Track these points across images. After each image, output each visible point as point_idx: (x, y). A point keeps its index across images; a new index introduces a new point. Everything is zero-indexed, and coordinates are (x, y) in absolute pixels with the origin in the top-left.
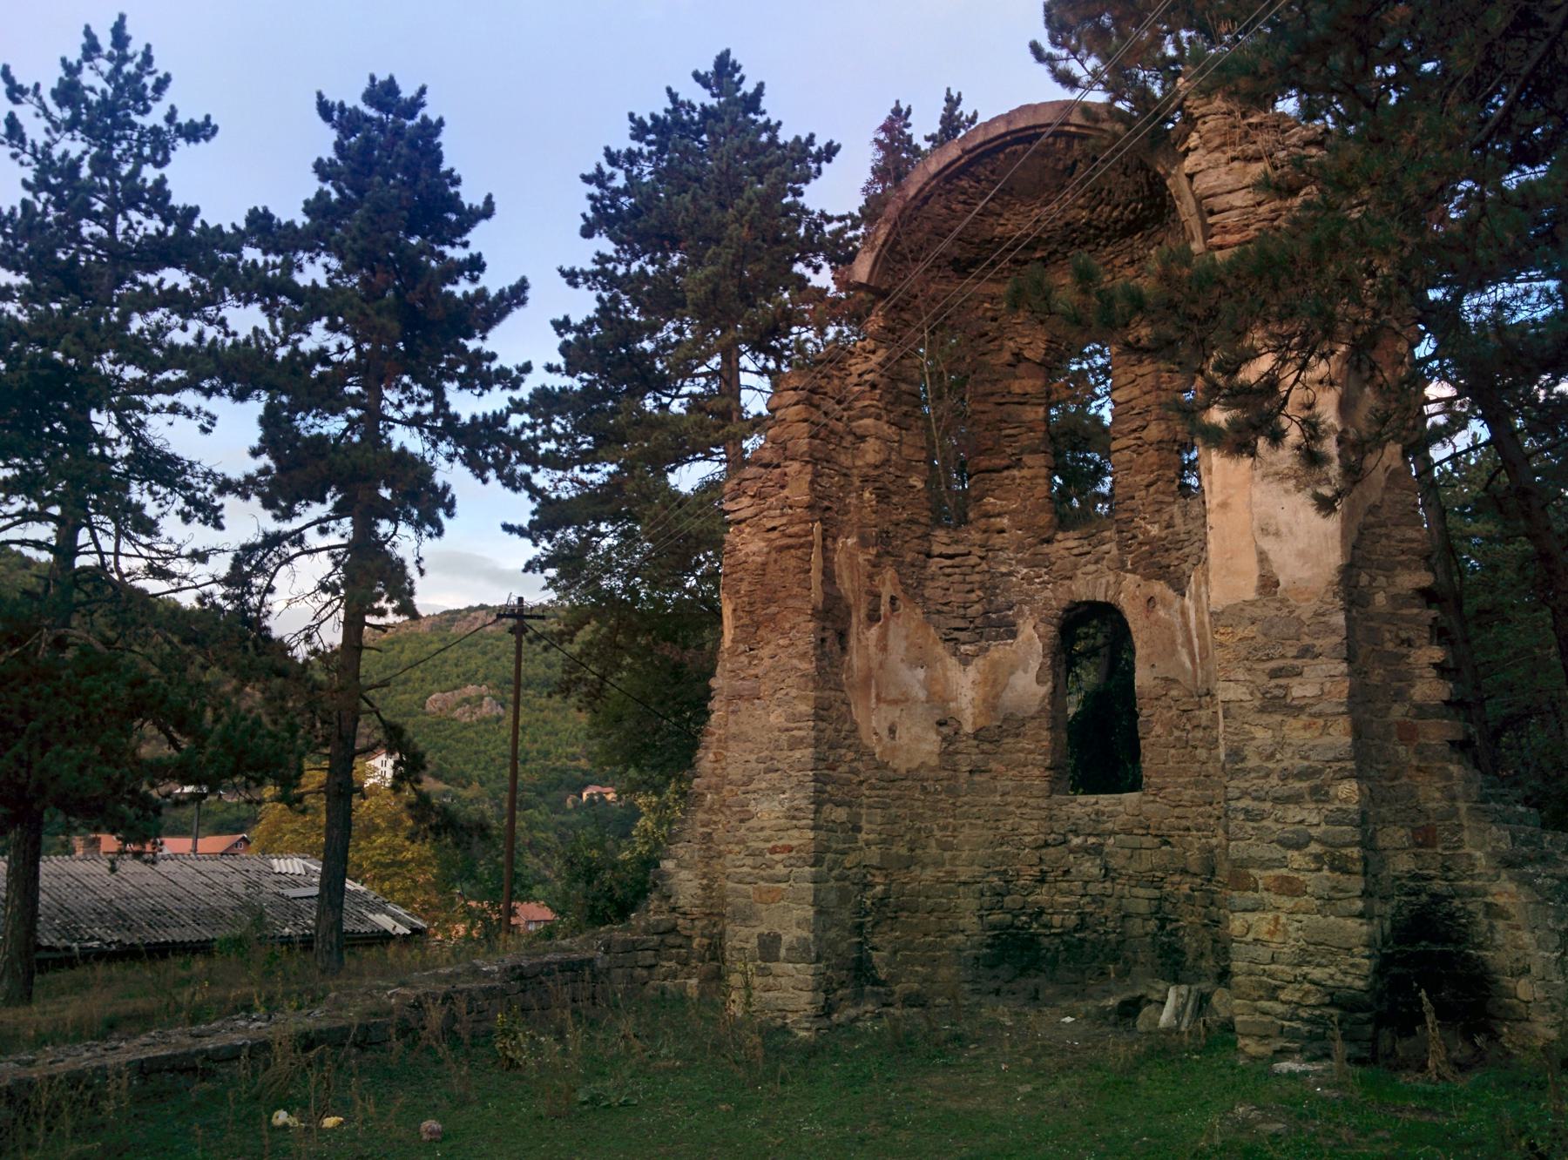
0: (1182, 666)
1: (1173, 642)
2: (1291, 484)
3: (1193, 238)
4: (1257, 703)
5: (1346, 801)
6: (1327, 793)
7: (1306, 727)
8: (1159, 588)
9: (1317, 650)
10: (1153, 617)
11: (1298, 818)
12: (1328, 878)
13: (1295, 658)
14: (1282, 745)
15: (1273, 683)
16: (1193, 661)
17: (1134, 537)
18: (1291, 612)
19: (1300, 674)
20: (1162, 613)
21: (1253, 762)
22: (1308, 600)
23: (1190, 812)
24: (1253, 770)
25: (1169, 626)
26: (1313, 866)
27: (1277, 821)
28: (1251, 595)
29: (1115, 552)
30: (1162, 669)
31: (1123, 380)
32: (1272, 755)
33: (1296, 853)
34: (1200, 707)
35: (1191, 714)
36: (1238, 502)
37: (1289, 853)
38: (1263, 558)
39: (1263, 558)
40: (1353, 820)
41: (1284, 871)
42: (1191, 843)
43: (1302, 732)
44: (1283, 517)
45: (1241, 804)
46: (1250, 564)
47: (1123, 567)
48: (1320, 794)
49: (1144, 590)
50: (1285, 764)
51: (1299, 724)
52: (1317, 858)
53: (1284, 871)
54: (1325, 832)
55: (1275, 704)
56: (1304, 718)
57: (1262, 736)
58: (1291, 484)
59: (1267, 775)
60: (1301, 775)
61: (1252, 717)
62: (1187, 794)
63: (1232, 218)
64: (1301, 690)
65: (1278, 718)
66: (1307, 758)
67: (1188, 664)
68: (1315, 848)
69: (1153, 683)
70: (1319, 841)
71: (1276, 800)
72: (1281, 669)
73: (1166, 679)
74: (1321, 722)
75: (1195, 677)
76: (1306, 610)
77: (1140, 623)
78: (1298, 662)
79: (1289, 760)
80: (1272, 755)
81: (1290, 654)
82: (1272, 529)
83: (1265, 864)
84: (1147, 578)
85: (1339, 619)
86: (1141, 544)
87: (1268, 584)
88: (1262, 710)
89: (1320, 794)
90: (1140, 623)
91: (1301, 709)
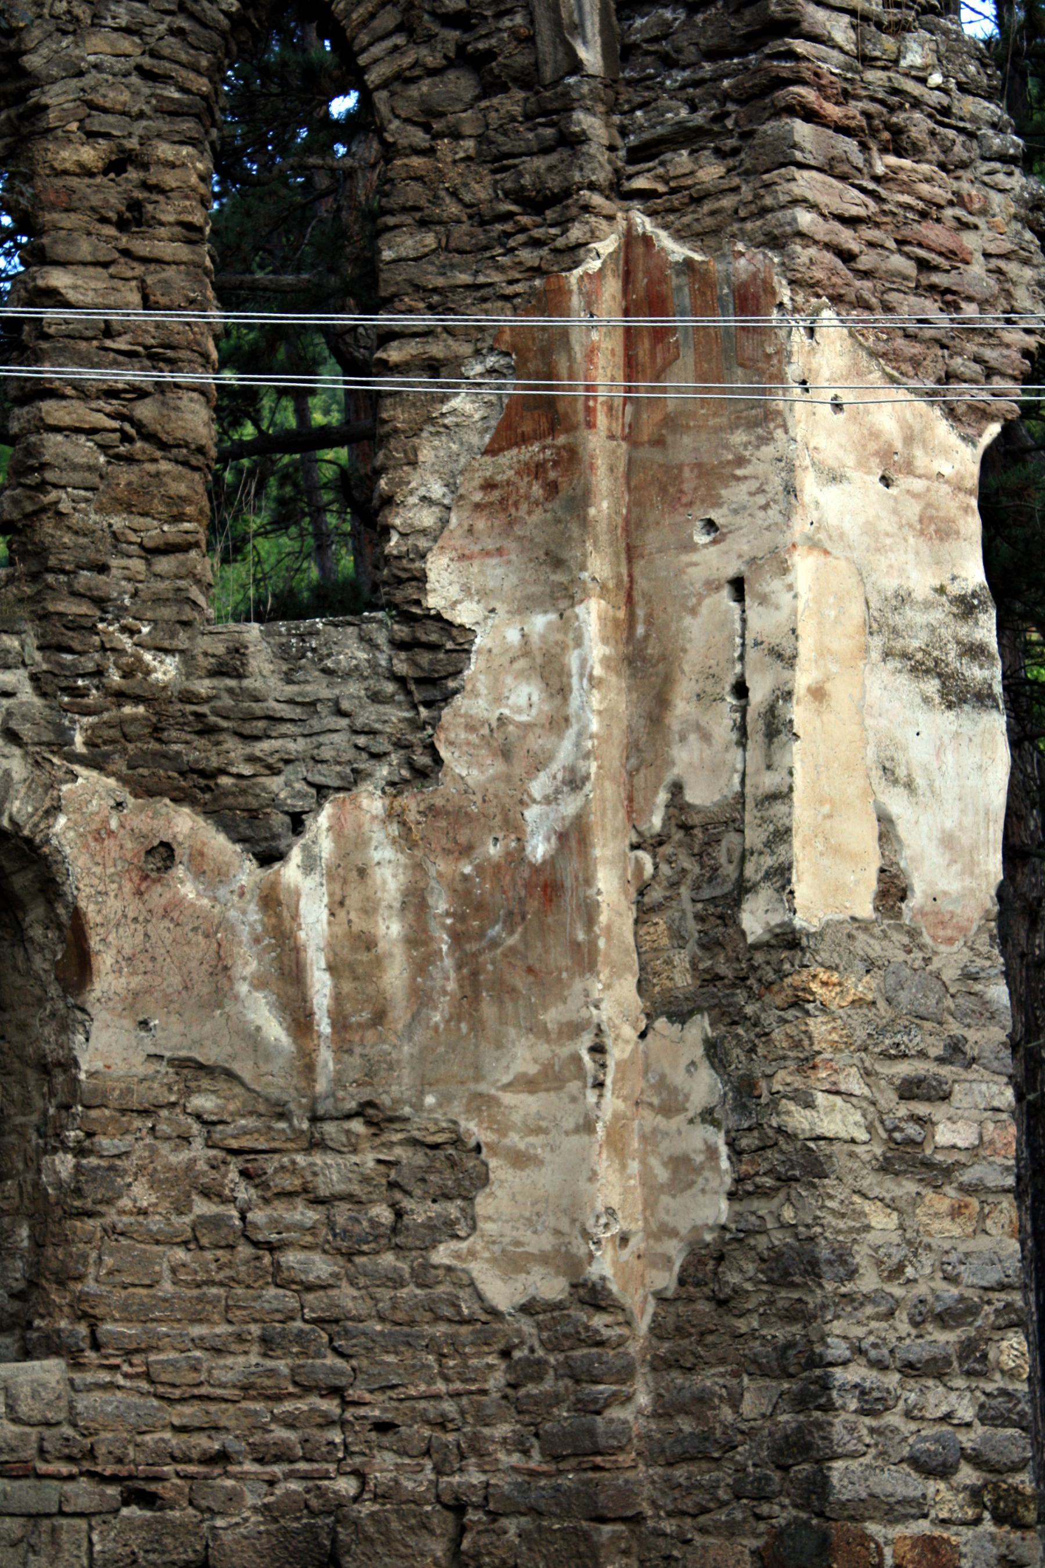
0: (253, 1038)
1: (221, 968)
2: (932, 686)
3: (578, 28)
4: (878, 1150)
5: (1012, 1374)
6: (985, 1356)
7: (956, 1212)
8: (184, 823)
9: (971, 1051)
10: (158, 896)
11: (944, 1409)
12: (993, 1538)
13: (941, 1060)
14: (915, 1247)
15: (903, 1110)
16: (300, 1022)
17: (99, 673)
18: (927, 960)
19: (946, 1097)
20: (189, 891)
21: (868, 1282)
22: (950, 941)
23: (225, 1415)
24: (868, 1298)
25: (215, 930)
26: (970, 1513)
27: (908, 1415)
28: (866, 910)
29: (27, 693)
30: (173, 1035)
31: (84, 248)
32: (900, 1269)
33: (942, 1486)
34: (316, 1144)
35: (270, 1165)
36: (840, 691)
37: (933, 1486)
38: (886, 829)
39: (886, 829)
40: (1022, 1415)
41: (923, 1526)
42: (233, 1497)
43: (947, 1223)
44: (918, 754)
45: (855, 1374)
46: (863, 834)
47: (60, 743)
48: (973, 1358)
49: (141, 822)
50: (922, 1289)
51: (943, 1205)
52: (975, 1494)
53: (923, 1526)
54: (985, 1440)
55: (905, 1155)
56: (950, 1190)
57: (882, 1222)
58: (932, 686)
59: (891, 1314)
60: (945, 1319)
61: (869, 1181)
62: (244, 1362)
63: (831, 64)
64: (951, 1133)
65: (910, 1187)
66: (952, 1279)
67: (275, 1030)
68: (967, 1475)
69: (142, 1069)
70: (976, 1460)
71: (910, 1369)
72: (919, 1082)
73: (181, 1064)
74: (974, 1203)
75: (309, 1069)
76: (950, 959)
77: (113, 905)
78: (945, 1071)
79: (926, 1283)
80: (900, 1269)
81: (935, 1051)
82: (901, 772)
83: (894, 1511)
84: (146, 791)
85: (999, 993)
86: (121, 696)
87: (892, 890)
88: (885, 1167)
89: (973, 1358)
90: (113, 905)
91: (947, 1171)
